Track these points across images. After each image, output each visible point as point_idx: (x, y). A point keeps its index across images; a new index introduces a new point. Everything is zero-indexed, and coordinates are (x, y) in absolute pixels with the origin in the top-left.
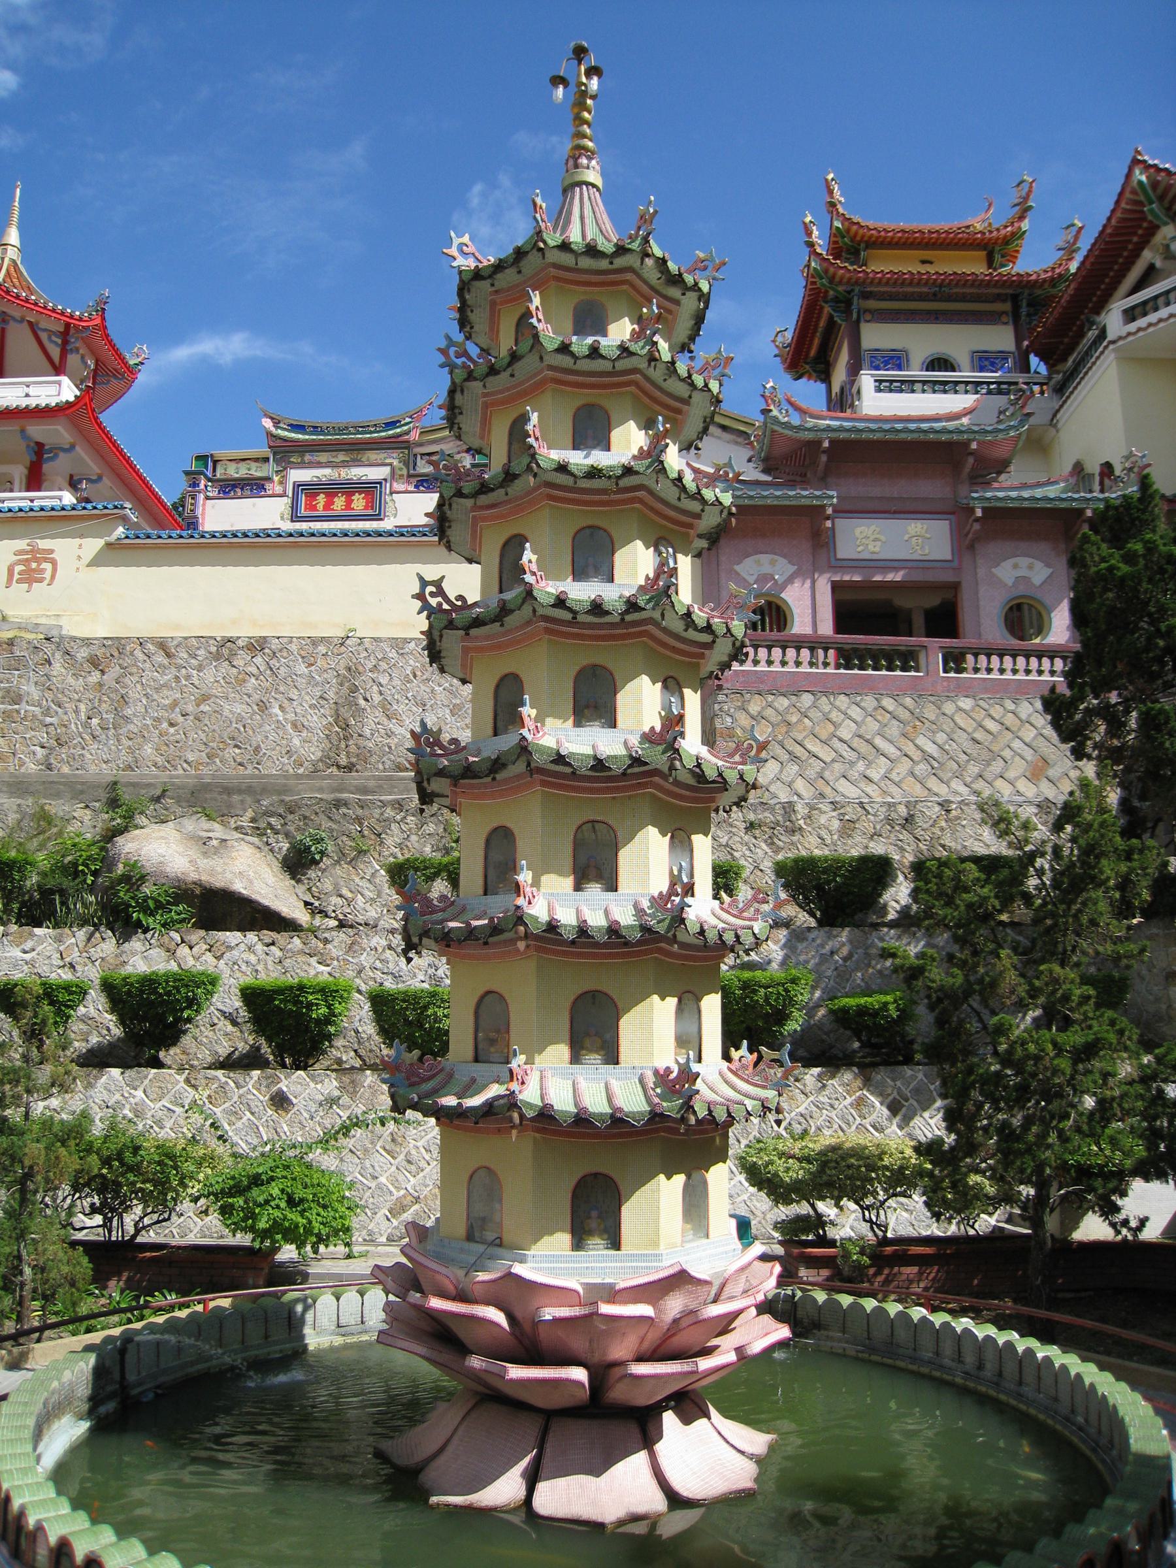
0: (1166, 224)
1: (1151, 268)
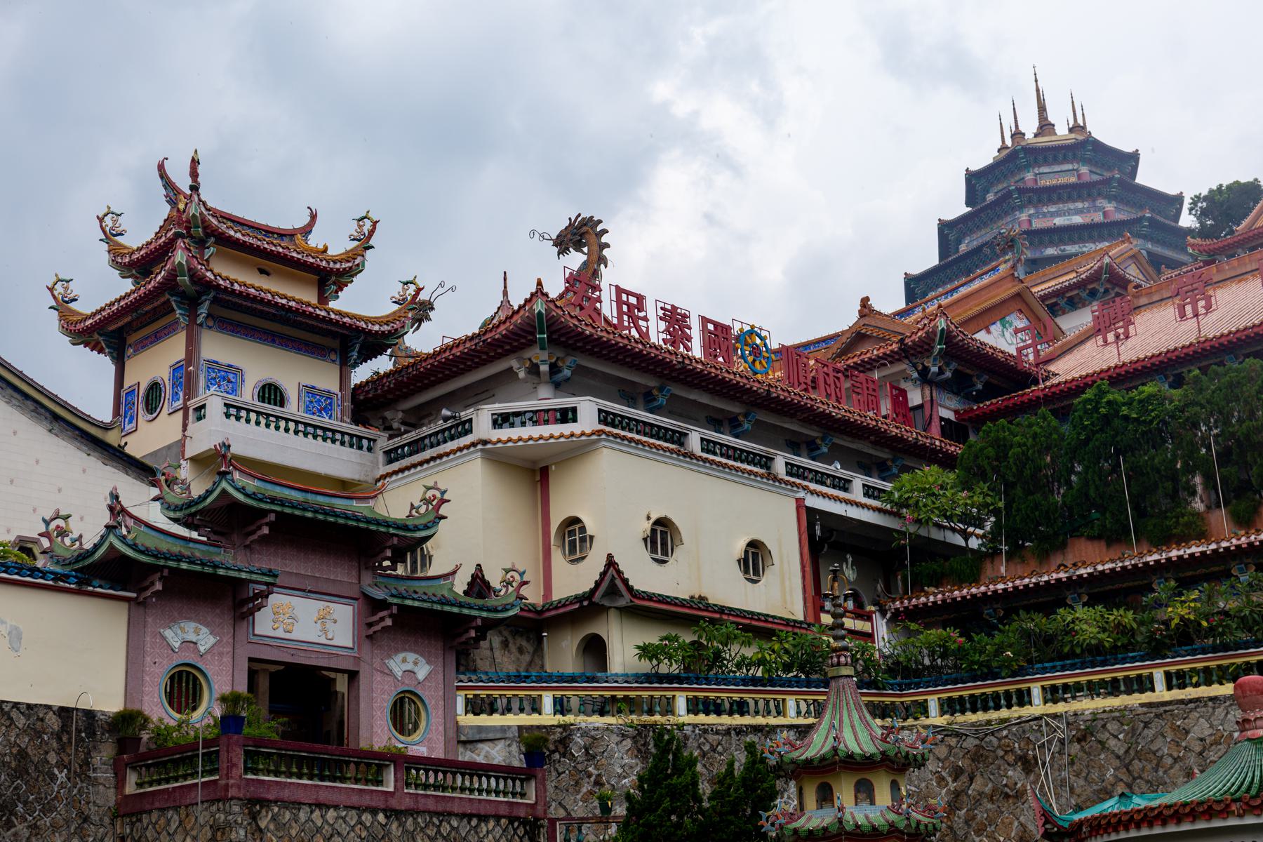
0: (542, 348)
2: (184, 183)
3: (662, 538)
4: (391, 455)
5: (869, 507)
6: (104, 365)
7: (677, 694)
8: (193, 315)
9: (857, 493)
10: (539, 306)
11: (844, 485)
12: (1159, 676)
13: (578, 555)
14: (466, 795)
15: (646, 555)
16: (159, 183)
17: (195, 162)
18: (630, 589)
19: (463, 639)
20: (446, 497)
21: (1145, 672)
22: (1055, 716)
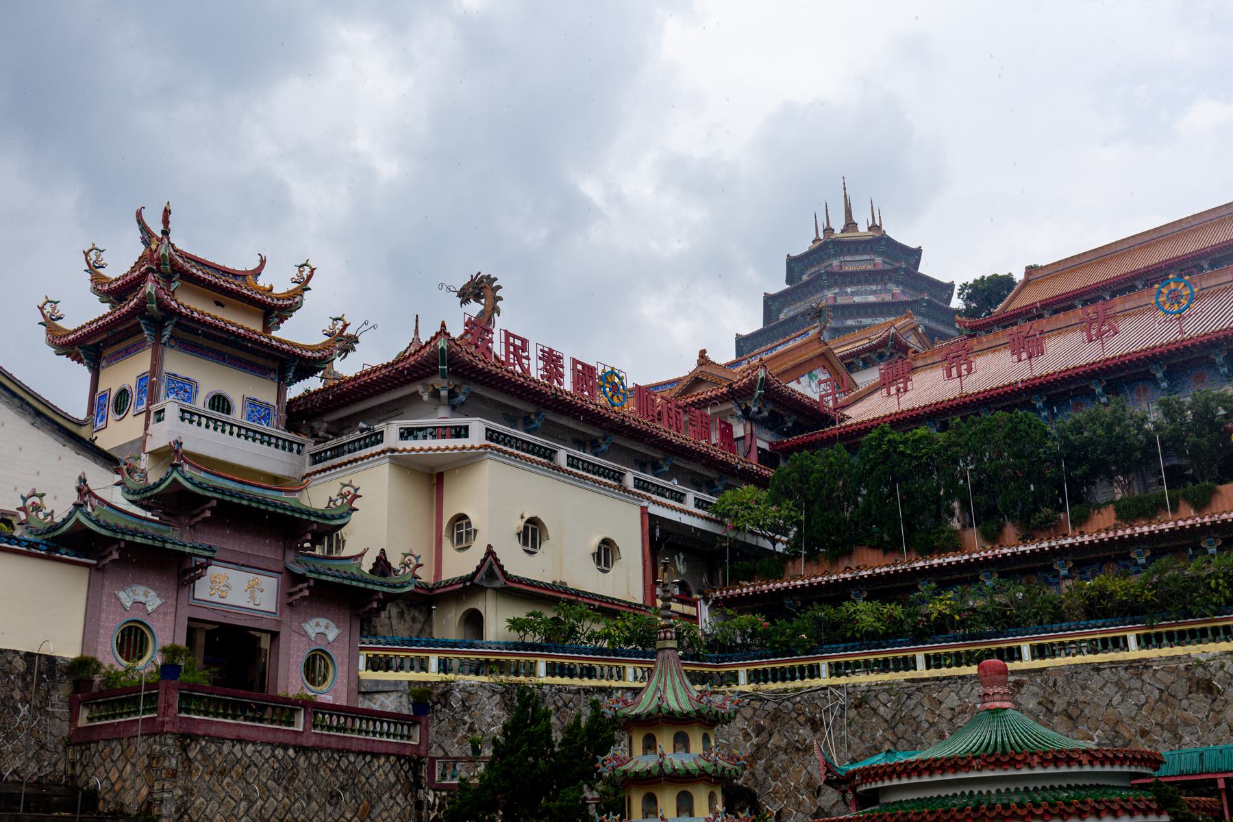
0: (444, 377)
1: (416, 396)
2: (157, 228)
3: (532, 533)
4: (316, 458)
5: (698, 516)
6: (82, 373)
7: (539, 659)
8: (158, 335)
9: (690, 504)
10: (442, 343)
11: (680, 497)
12: (920, 658)
13: (464, 545)
14: (362, 736)
15: (518, 547)
16: (137, 227)
17: (167, 212)
18: (504, 573)
19: (367, 609)
20: (358, 493)
21: (910, 654)
22: (838, 687)
